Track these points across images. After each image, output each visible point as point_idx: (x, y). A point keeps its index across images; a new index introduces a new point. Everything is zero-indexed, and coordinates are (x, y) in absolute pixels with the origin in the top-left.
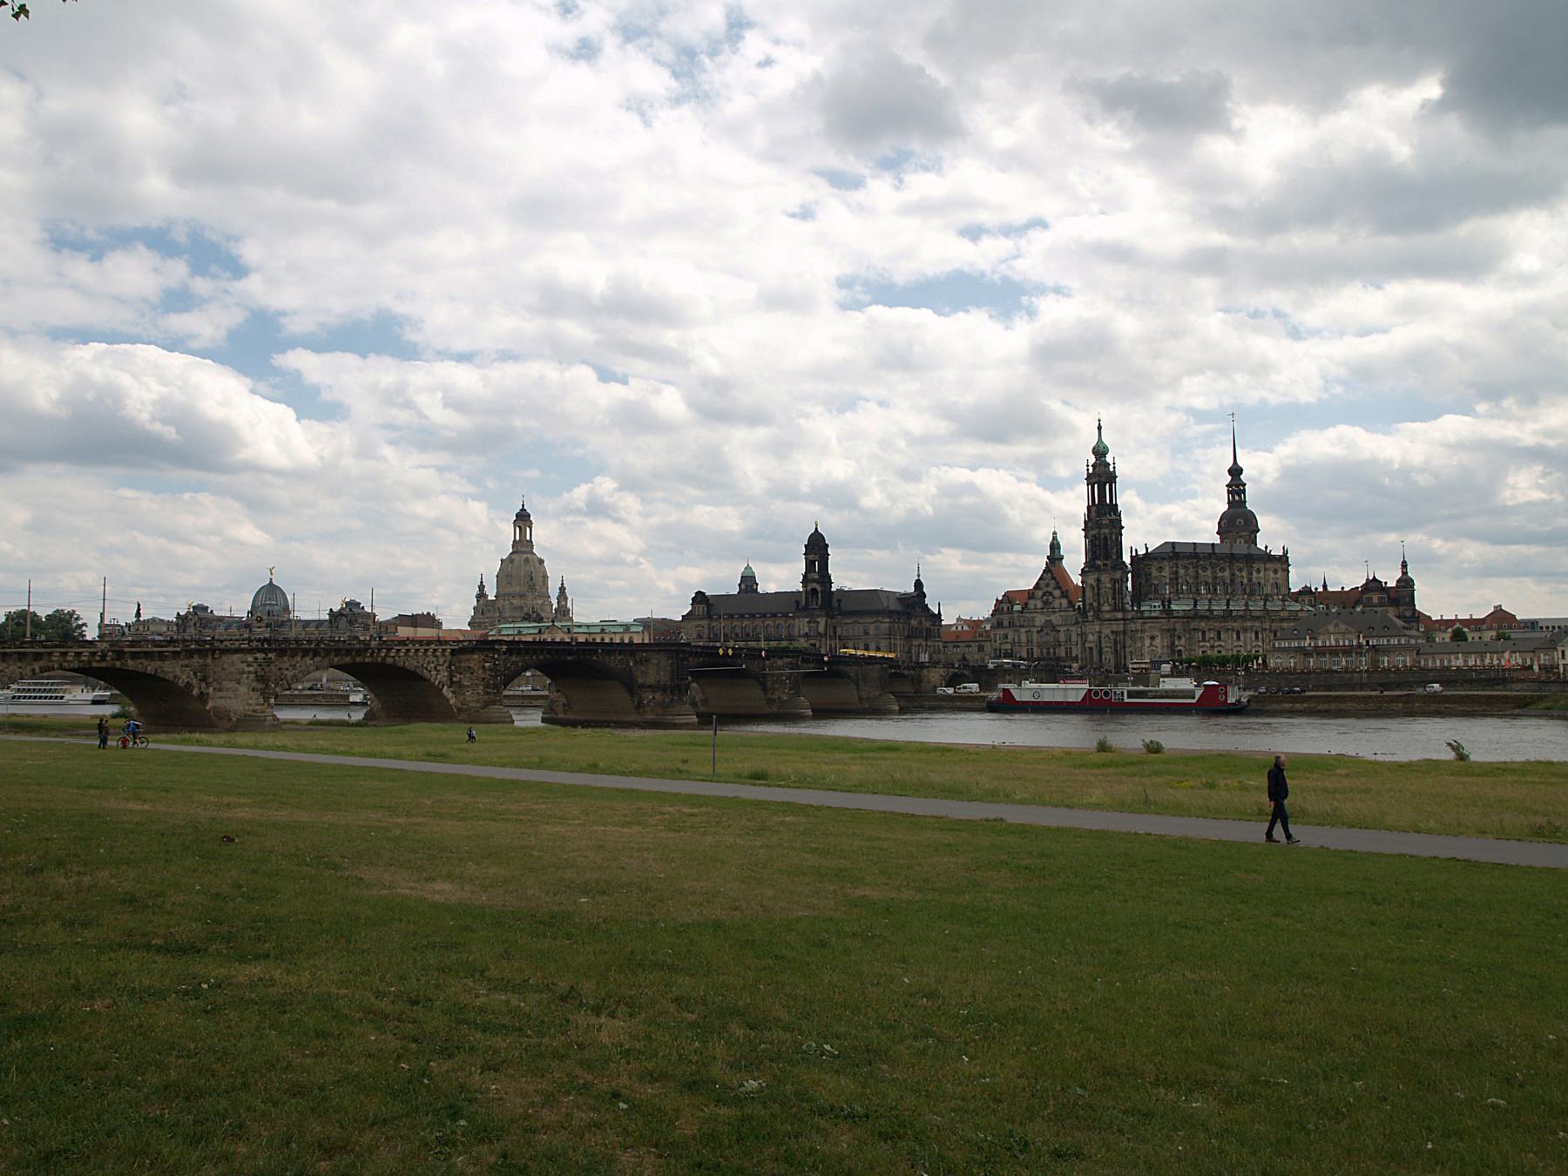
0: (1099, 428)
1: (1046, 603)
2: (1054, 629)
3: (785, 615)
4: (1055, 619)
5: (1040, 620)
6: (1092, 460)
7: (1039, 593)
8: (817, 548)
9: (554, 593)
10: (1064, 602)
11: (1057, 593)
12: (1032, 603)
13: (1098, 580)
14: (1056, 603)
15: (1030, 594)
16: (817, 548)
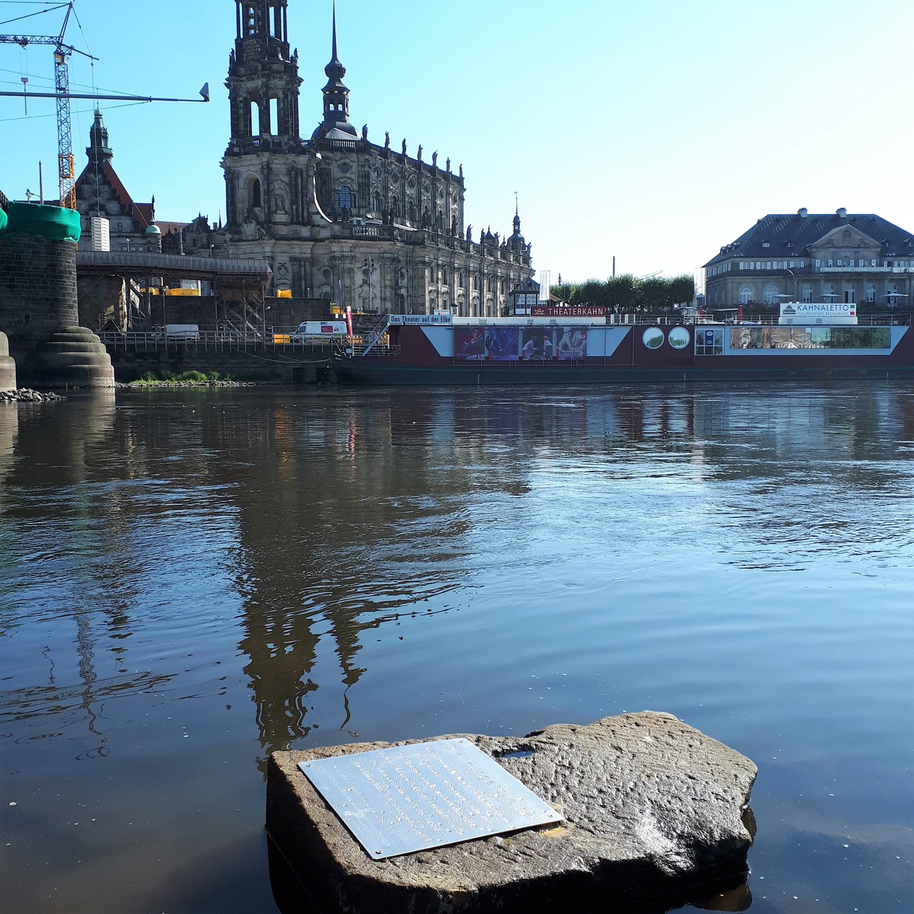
13: (269, 169)
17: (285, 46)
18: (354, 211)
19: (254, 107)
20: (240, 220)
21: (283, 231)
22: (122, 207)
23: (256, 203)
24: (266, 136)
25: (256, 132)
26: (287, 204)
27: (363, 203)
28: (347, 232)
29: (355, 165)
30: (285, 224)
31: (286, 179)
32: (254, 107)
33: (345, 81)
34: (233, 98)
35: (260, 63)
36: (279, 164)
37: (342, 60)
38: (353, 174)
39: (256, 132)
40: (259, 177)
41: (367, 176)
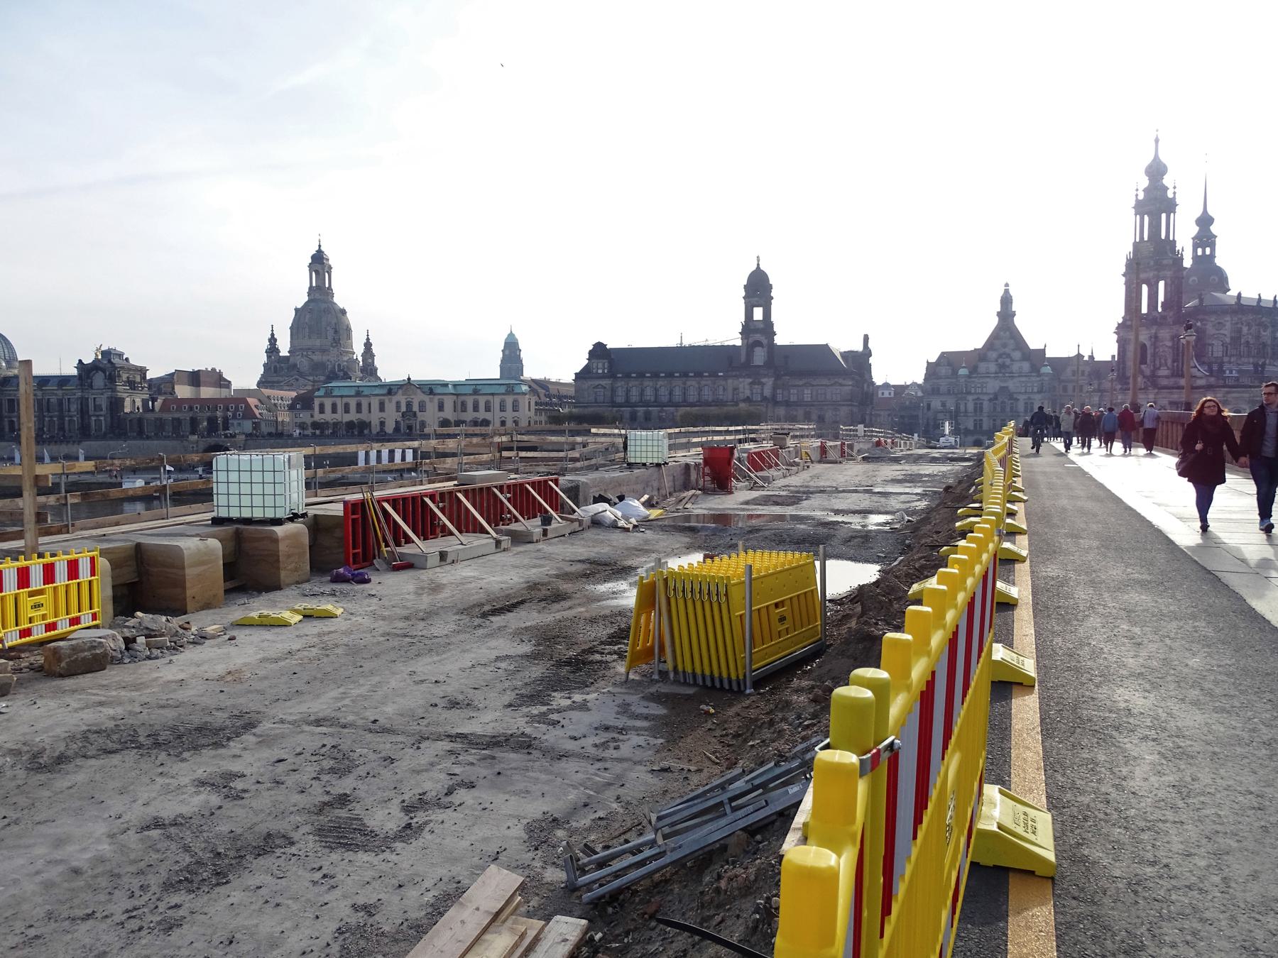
0: (1157, 141)
1: (1002, 366)
2: (1011, 396)
3: (714, 375)
4: (1012, 385)
5: (993, 385)
6: (1145, 182)
7: (993, 355)
8: (758, 289)
9: (358, 349)
10: (1026, 366)
11: (1017, 355)
12: (983, 367)
13: (1156, 337)
14: (1015, 367)
15: (978, 356)
16: (758, 289)
17: (1174, 241)
18: (1226, 359)
19: (1145, 288)
20: (1130, 373)
21: (1164, 382)
22: (1023, 354)
23: (1143, 361)
24: (1154, 314)
25: (1144, 310)
26: (1169, 362)
27: (1234, 352)
28: (1221, 382)
29: (1228, 324)
30: (1167, 377)
31: (1169, 344)
32: (1145, 288)
33: (1214, 229)
34: (1128, 285)
35: (1153, 257)
36: (1165, 334)
37: (1211, 212)
38: (1227, 331)
39: (1144, 310)
40: (1148, 344)
41: (1240, 331)
